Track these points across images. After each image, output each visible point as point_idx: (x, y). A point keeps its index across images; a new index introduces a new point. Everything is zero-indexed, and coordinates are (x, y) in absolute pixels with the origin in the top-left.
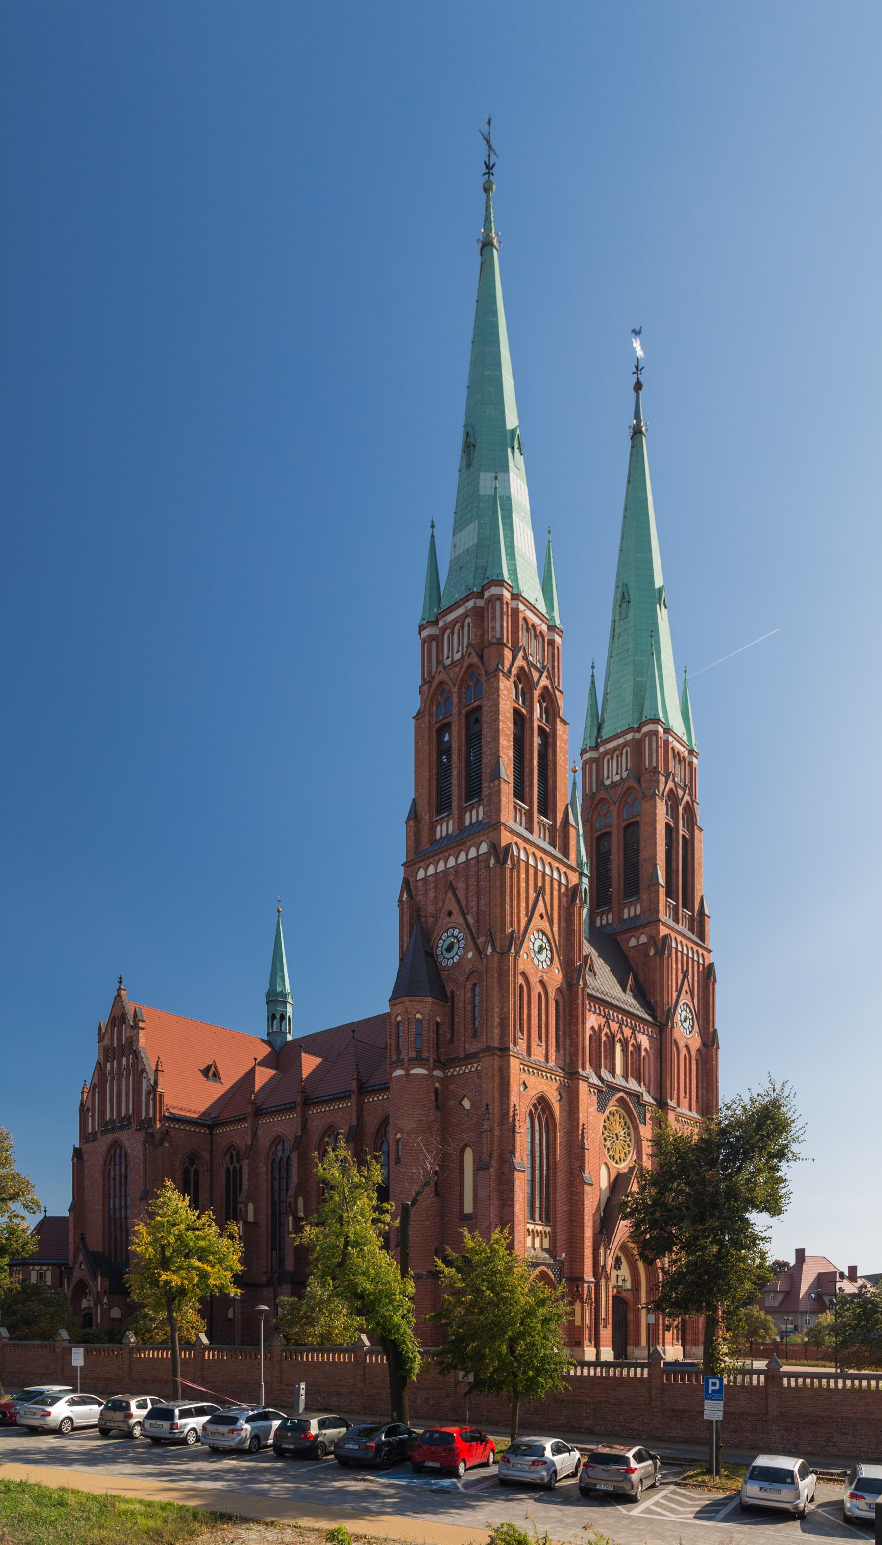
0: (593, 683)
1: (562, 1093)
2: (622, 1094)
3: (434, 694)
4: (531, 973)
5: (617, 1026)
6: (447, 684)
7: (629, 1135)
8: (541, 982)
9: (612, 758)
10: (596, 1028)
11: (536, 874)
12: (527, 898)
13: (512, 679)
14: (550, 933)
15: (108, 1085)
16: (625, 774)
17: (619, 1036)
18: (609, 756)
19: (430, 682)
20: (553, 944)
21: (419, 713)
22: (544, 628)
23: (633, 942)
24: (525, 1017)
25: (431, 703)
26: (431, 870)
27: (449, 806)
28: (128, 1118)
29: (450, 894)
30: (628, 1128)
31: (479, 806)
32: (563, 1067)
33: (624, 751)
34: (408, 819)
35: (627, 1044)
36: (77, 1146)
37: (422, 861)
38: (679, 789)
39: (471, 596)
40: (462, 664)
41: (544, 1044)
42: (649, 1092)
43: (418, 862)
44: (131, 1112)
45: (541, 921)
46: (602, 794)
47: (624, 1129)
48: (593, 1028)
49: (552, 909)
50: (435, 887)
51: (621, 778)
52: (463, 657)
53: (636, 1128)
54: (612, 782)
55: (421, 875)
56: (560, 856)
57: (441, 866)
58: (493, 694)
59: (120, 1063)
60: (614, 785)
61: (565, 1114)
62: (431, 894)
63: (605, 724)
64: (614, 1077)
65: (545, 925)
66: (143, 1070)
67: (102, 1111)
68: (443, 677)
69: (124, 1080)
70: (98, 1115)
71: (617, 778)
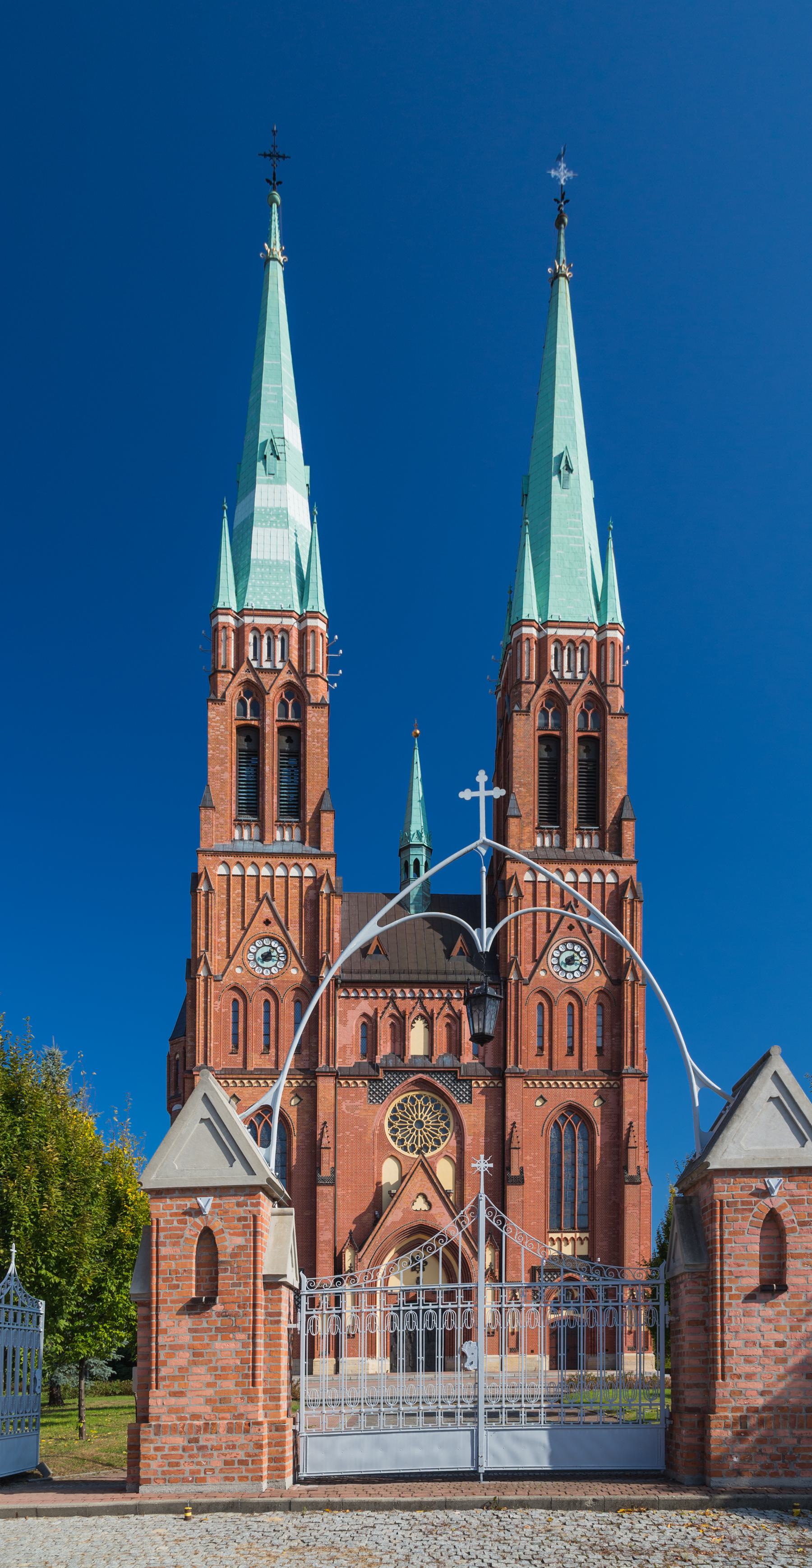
1: (300, 1095)
2: (420, 1075)
5: (412, 1003)
7: (444, 1118)
8: (267, 989)
10: (371, 1013)
14: (282, 935)
17: (419, 1010)
20: (287, 946)
24: (241, 1030)
30: (444, 1110)
32: (307, 1066)
35: (432, 1018)
41: (272, 1051)
42: (483, 1064)
45: (266, 927)
47: (434, 1113)
48: (365, 1015)
53: (454, 1109)
56: (307, 848)
61: (306, 1116)
64: (403, 1060)
65: (275, 929)
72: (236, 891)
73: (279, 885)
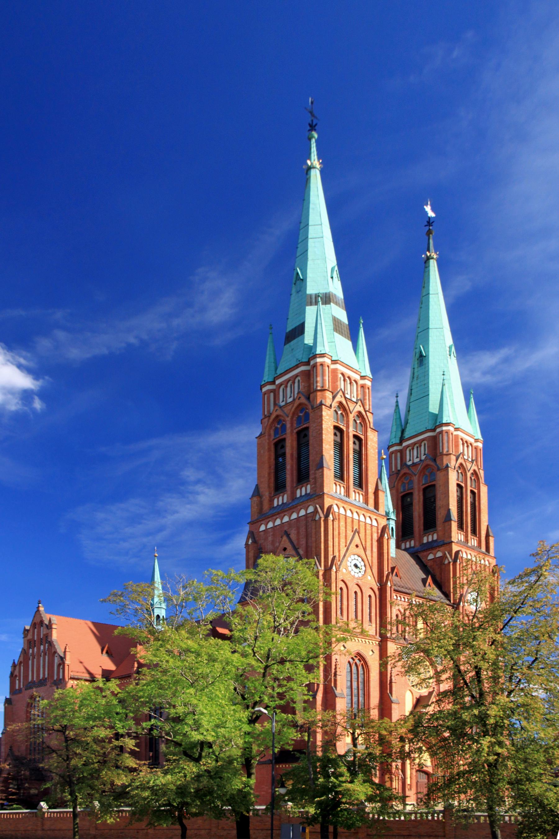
0: (397, 406)
3: (273, 422)
4: (349, 580)
6: (283, 417)
9: (413, 449)
11: (352, 521)
12: (346, 536)
13: (333, 409)
15: (30, 662)
16: (423, 457)
18: (410, 448)
19: (269, 417)
21: (261, 435)
22: (357, 377)
23: (431, 557)
25: (271, 428)
26: (270, 525)
27: (284, 486)
28: (45, 680)
29: (285, 538)
31: (307, 485)
33: (423, 444)
34: (253, 496)
36: (8, 697)
37: (263, 520)
38: (467, 464)
39: (300, 365)
40: (294, 404)
43: (260, 521)
44: (46, 676)
46: (405, 470)
49: (366, 541)
50: (273, 535)
51: (421, 460)
52: (294, 400)
54: (413, 463)
55: (263, 528)
57: (278, 522)
58: (317, 419)
59: (39, 649)
60: (414, 465)
62: (270, 539)
63: (407, 429)
65: (360, 551)
66: (55, 652)
67: (26, 677)
68: (279, 412)
69: (42, 658)
70: (23, 679)
71: (416, 460)
72: (342, 523)
73: (362, 524)
